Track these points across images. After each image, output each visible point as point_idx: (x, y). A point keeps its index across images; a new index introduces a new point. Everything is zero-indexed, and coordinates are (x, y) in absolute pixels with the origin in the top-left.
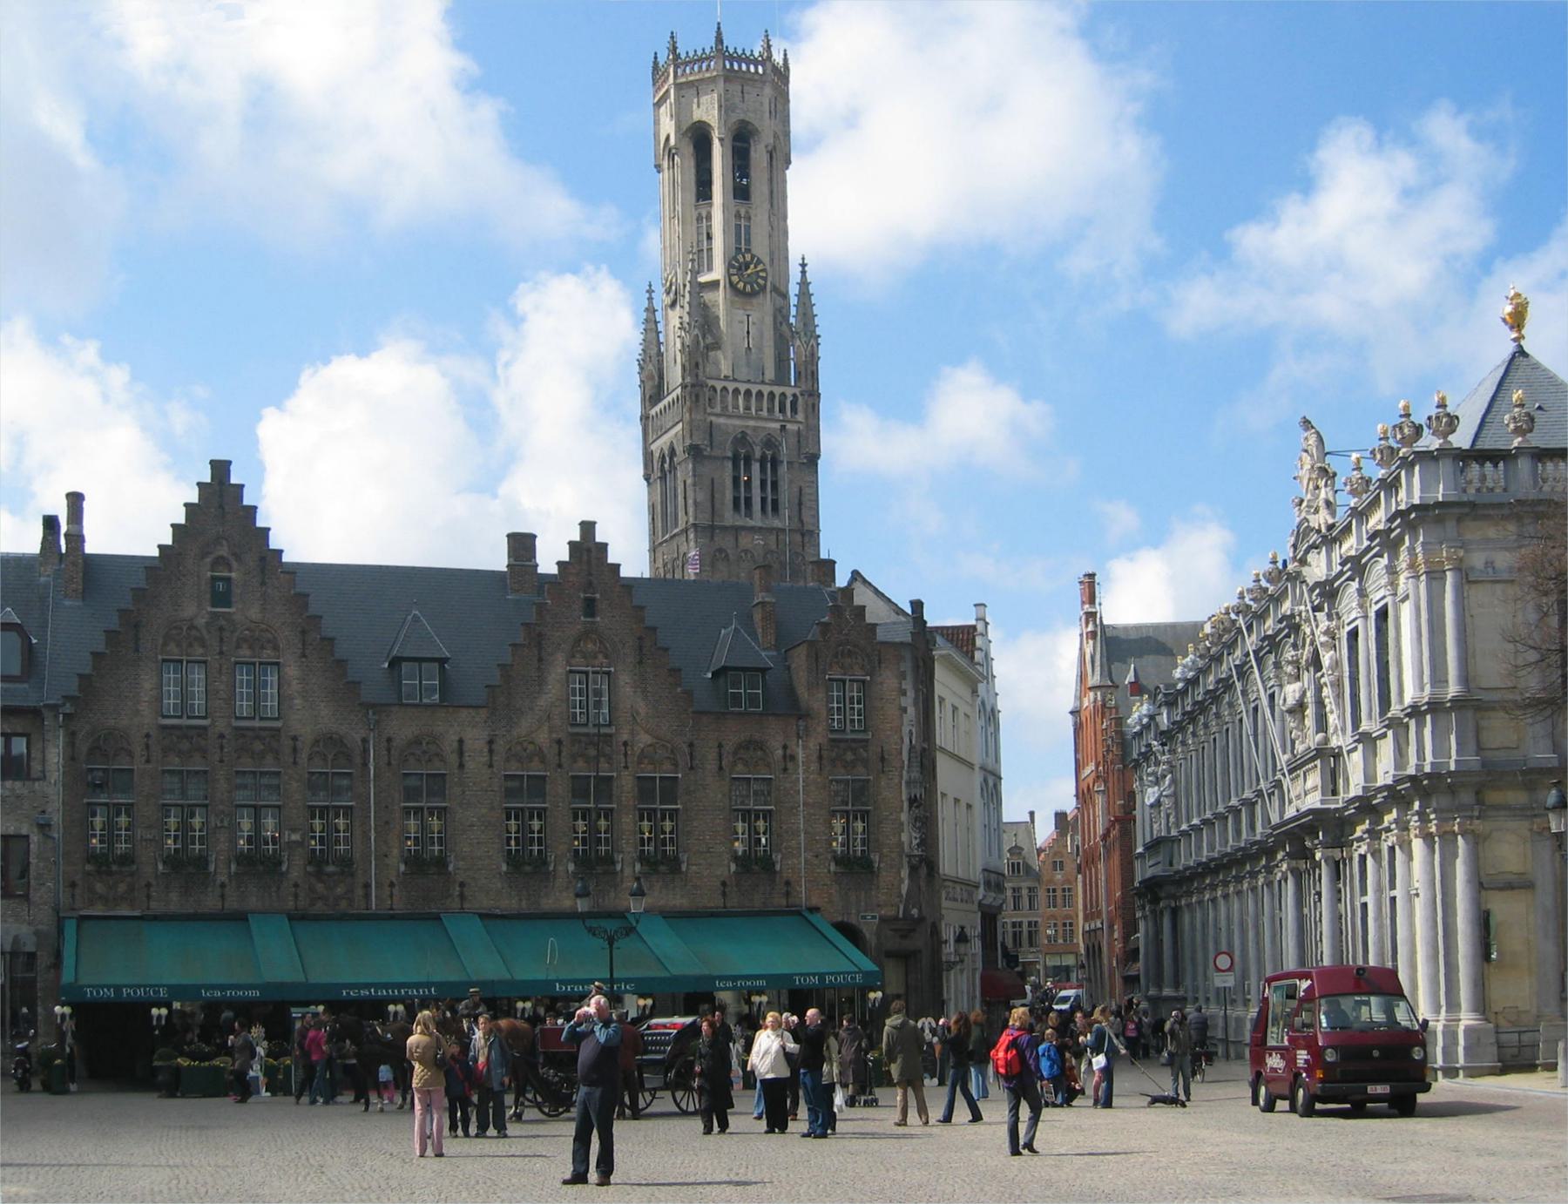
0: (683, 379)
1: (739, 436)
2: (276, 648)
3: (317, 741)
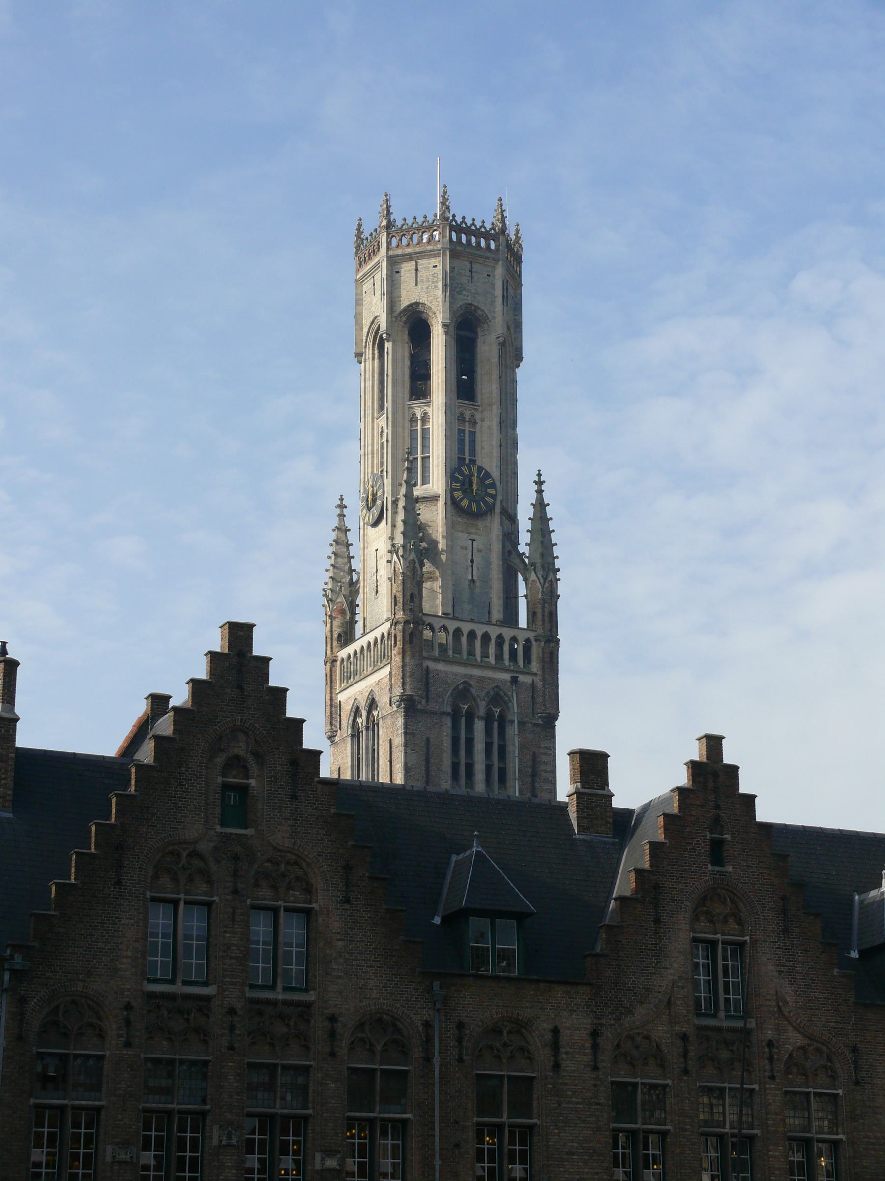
1: (461, 687)
2: (308, 890)
3: (361, 1026)
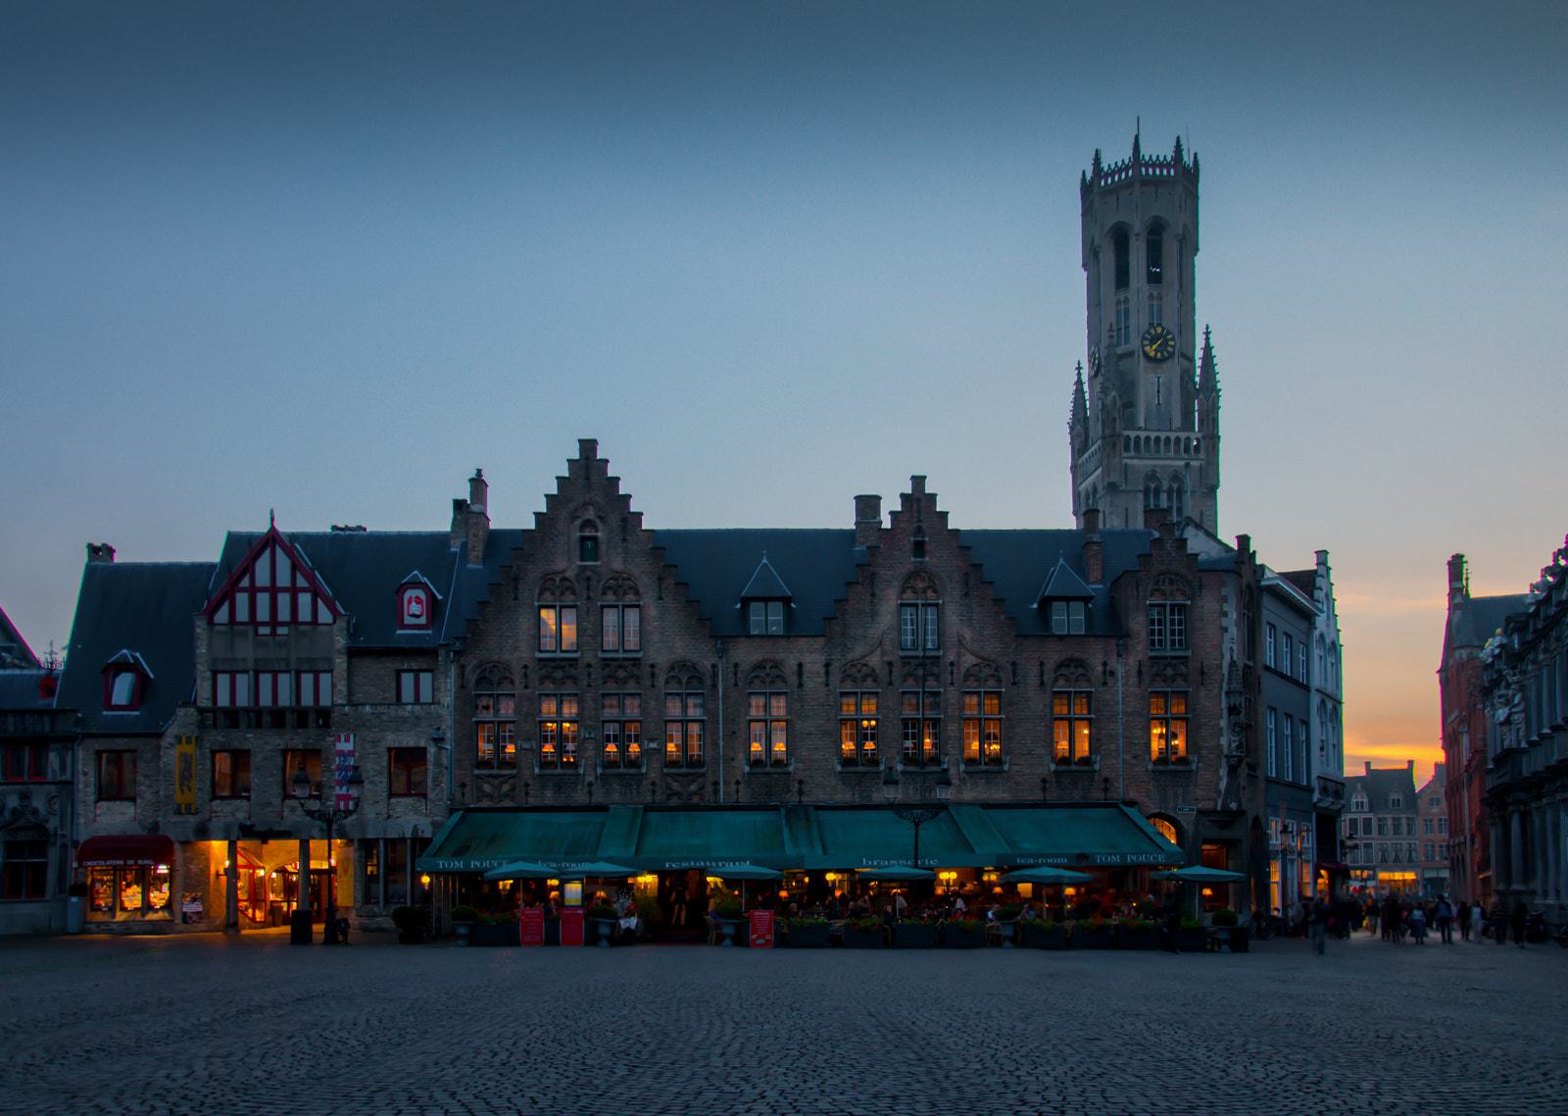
0: (1103, 431)
